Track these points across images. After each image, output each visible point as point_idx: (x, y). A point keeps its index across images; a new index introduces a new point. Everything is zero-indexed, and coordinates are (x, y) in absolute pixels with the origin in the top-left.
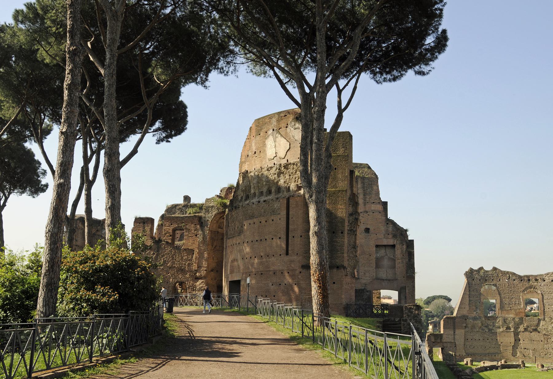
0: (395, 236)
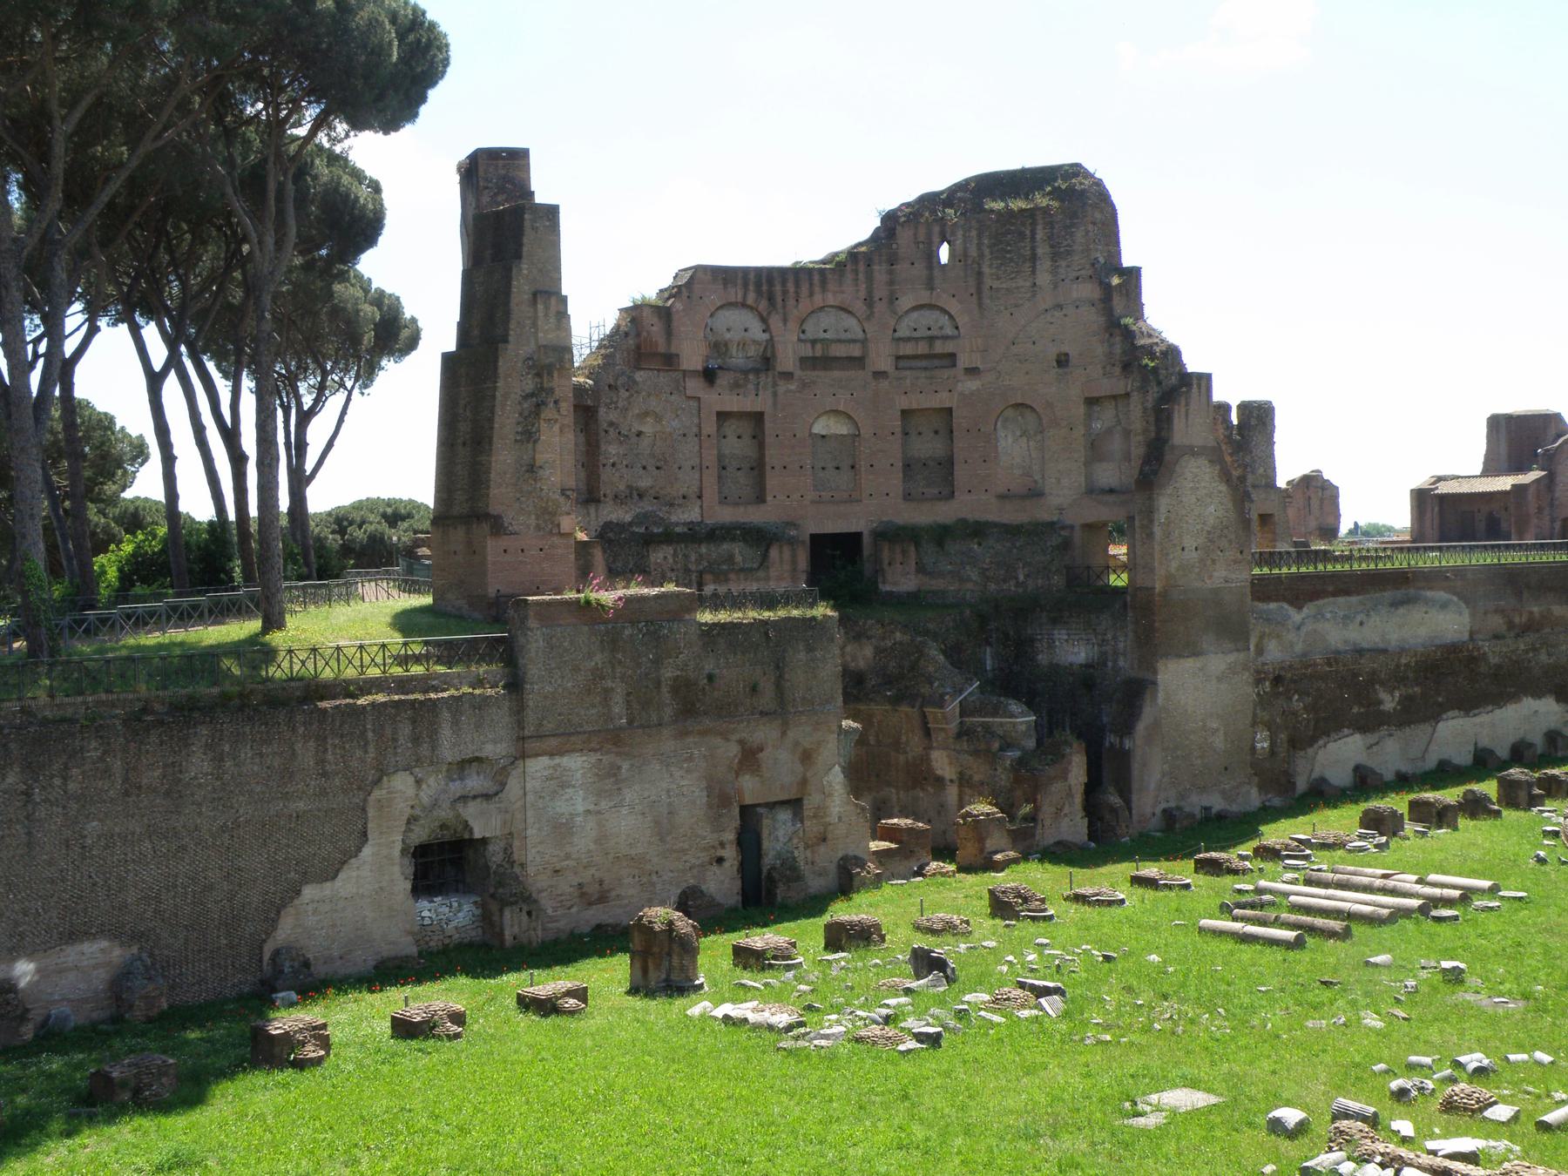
0: (1126, 367)
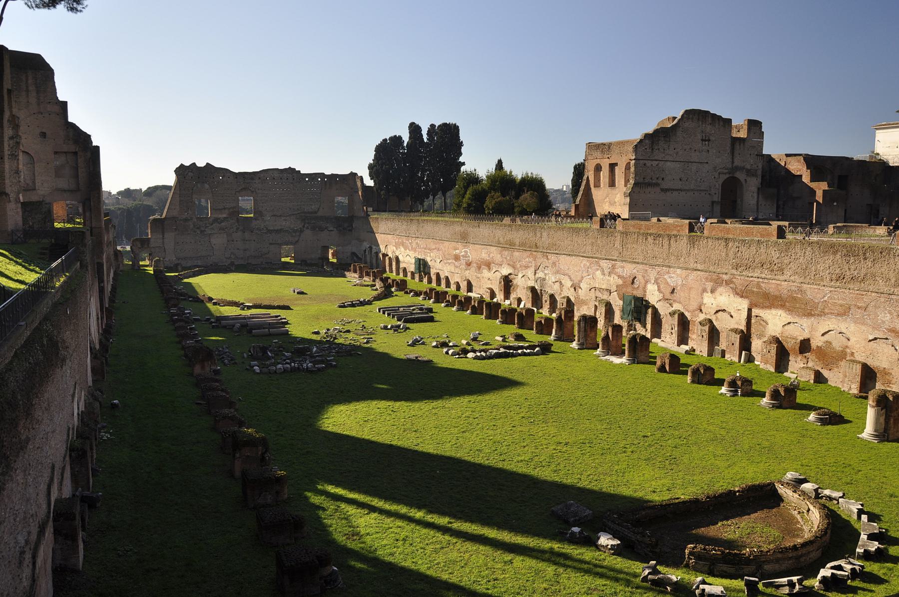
0: (76, 142)
